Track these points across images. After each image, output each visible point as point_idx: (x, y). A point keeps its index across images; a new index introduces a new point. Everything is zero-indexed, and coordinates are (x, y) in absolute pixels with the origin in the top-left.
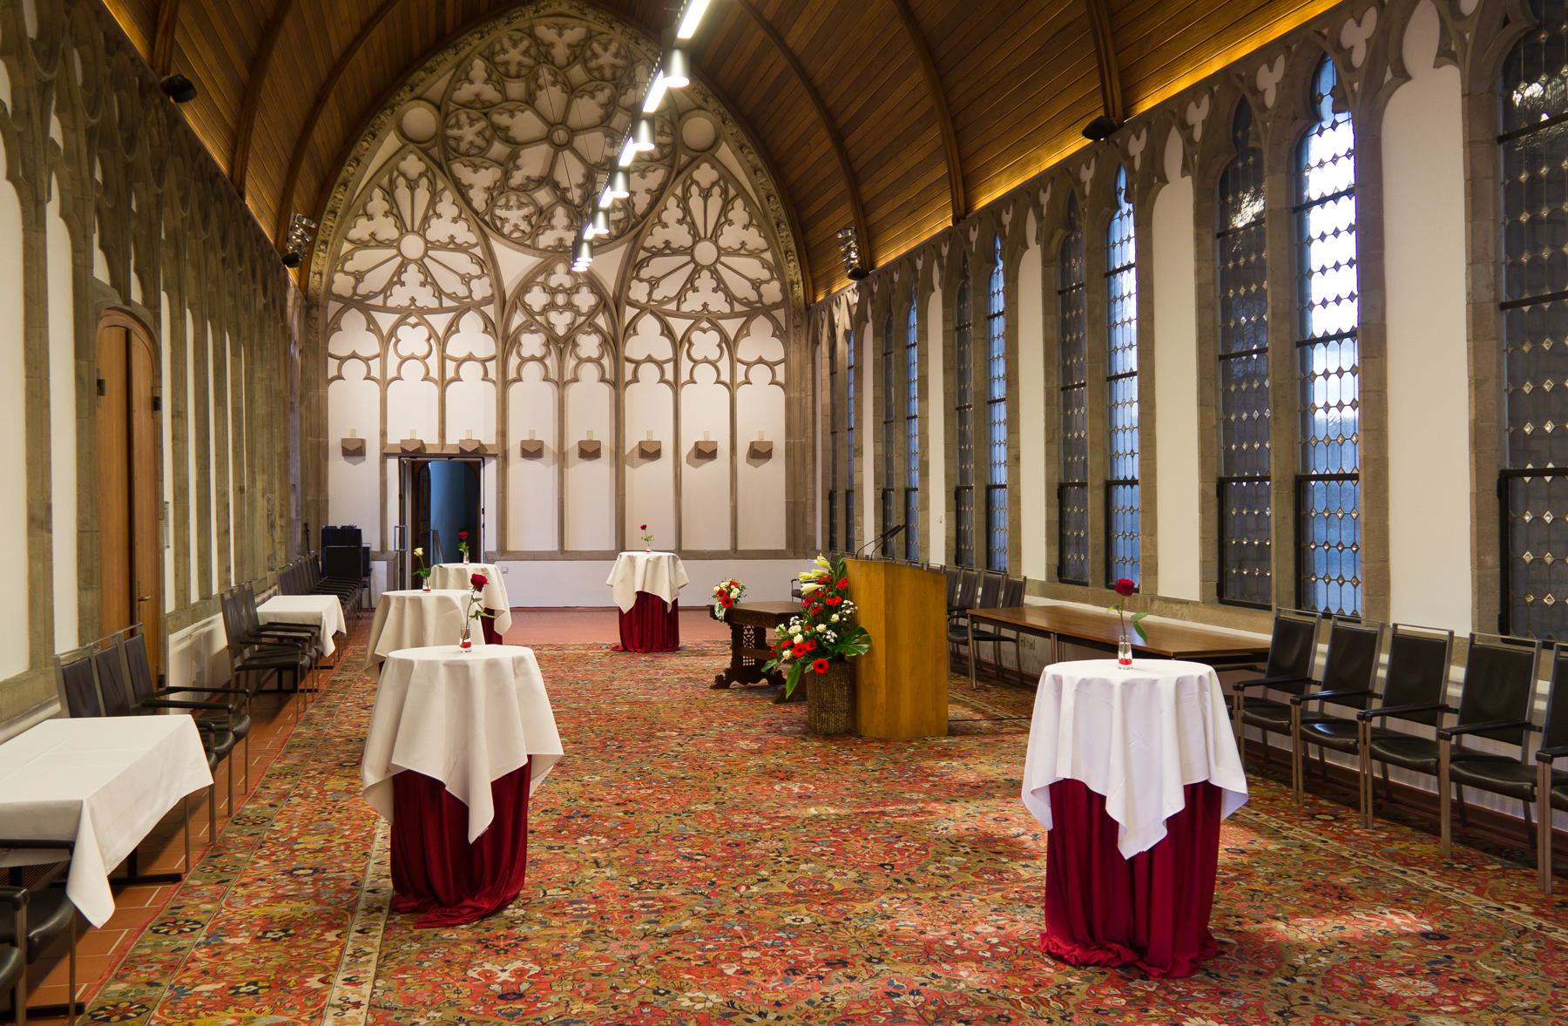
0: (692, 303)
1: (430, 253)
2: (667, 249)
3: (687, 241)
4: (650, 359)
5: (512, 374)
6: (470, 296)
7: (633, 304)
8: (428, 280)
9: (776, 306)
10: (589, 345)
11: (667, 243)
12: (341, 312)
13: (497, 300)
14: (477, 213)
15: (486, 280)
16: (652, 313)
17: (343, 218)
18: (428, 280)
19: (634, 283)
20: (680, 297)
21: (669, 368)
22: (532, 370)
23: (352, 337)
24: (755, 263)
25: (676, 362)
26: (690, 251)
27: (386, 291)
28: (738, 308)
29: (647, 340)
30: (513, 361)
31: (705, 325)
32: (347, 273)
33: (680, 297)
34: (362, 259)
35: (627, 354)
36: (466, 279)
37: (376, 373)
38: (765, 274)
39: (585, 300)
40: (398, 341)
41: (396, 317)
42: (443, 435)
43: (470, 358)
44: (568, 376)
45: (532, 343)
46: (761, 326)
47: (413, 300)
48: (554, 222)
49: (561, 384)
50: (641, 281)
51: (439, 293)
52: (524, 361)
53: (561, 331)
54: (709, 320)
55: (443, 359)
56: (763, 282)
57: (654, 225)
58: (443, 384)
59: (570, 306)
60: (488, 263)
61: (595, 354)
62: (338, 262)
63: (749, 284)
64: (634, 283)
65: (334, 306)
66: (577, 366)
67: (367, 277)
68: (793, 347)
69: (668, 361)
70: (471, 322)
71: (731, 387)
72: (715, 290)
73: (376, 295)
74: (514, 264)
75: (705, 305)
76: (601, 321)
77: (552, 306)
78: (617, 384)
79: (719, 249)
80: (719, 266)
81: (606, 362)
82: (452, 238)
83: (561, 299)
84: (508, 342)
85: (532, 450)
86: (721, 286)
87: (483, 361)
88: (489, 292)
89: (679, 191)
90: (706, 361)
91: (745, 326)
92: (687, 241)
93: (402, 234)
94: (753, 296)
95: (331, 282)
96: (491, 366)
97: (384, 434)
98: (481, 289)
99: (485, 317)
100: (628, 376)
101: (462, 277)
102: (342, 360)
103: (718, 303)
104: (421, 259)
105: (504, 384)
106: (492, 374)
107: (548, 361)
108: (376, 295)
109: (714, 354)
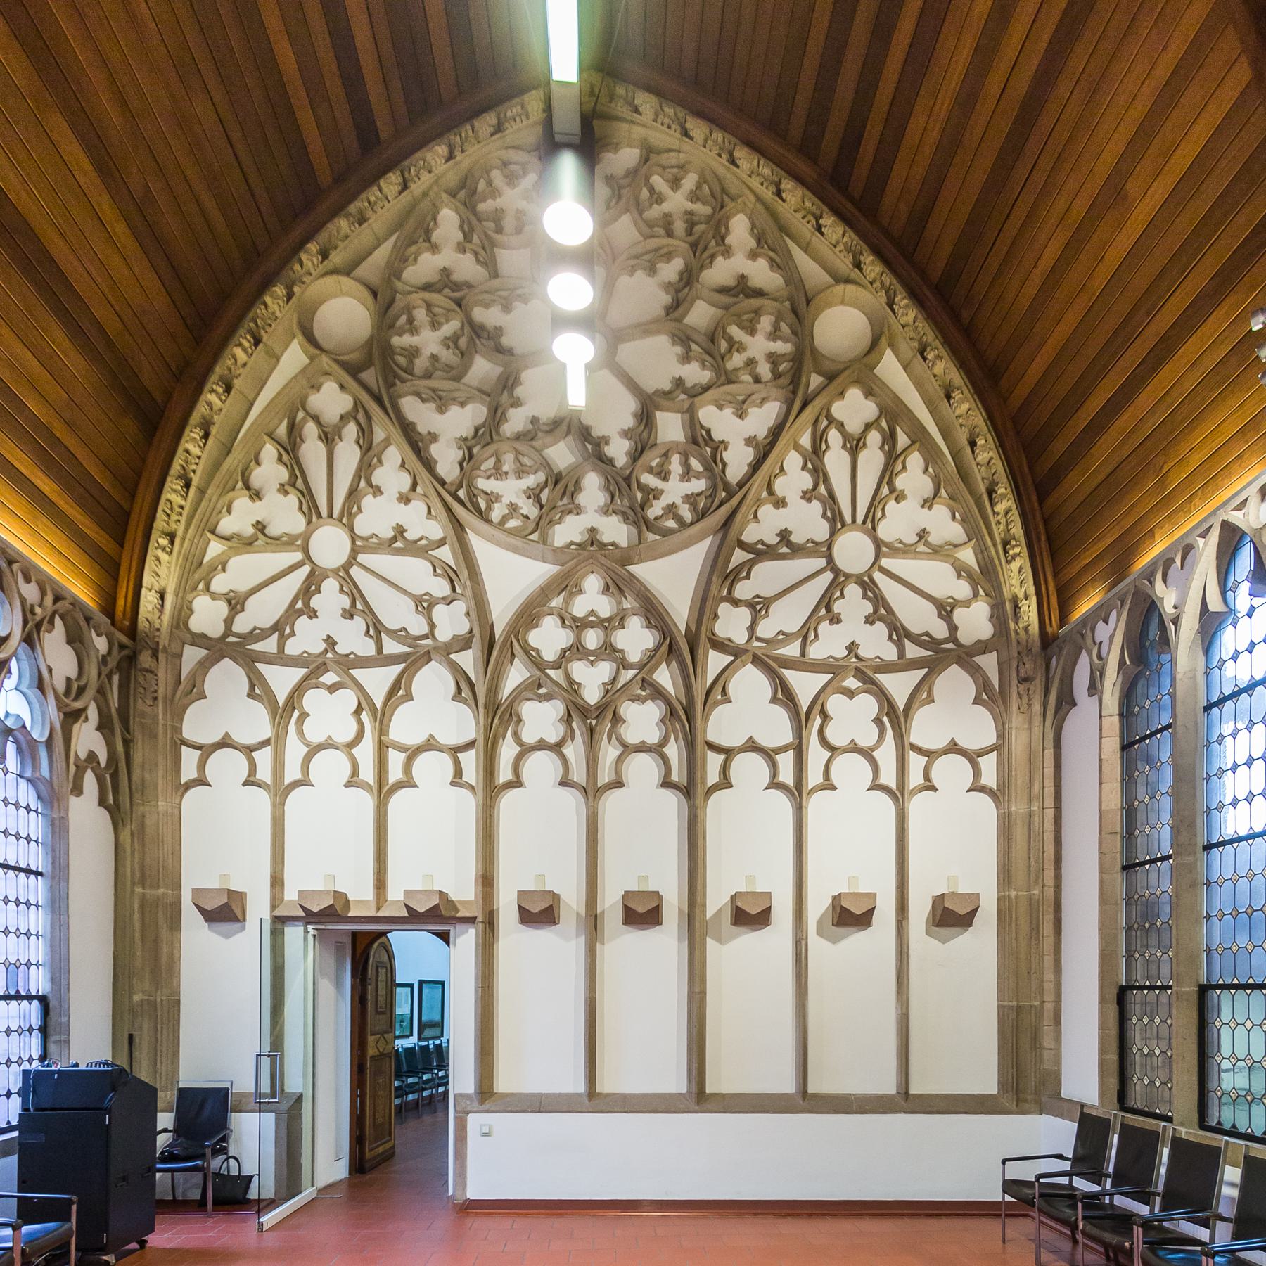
0: (830, 643)
1: (362, 558)
2: (785, 545)
3: (821, 531)
4: (752, 746)
5: (504, 774)
6: (431, 634)
7: (720, 645)
8: (357, 606)
9: (983, 647)
10: (642, 720)
11: (784, 535)
12: (204, 666)
13: (477, 642)
14: (443, 483)
15: (460, 606)
16: (757, 660)
17: (202, 492)
18: (357, 606)
19: (724, 608)
20: (806, 634)
21: (786, 762)
22: (541, 767)
23: (224, 708)
24: (945, 569)
25: (799, 750)
26: (825, 549)
27: (281, 628)
28: (913, 651)
29: (747, 711)
30: (507, 751)
31: (852, 683)
32: (214, 596)
33: (806, 634)
34: (243, 571)
35: (711, 737)
36: (425, 604)
37: (264, 773)
38: (962, 589)
39: (636, 639)
40: (304, 715)
41: (301, 672)
42: (381, 884)
43: (430, 745)
44: (604, 777)
45: (541, 719)
46: (954, 684)
47: (330, 642)
48: (581, 499)
49: (592, 792)
50: (736, 603)
51: (376, 629)
52: (526, 750)
53: (592, 695)
54: (859, 674)
55: (382, 748)
56: (955, 604)
57: (759, 502)
58: (383, 791)
59: (608, 650)
60: (465, 576)
61: (653, 737)
62: (197, 574)
63: (931, 609)
64: (724, 608)
65: (192, 655)
66: (620, 760)
67: (251, 603)
68: (1017, 720)
70: (433, 681)
71: (899, 795)
72: (870, 620)
73: (264, 634)
74: (509, 576)
75: (852, 647)
76: (665, 677)
77: (576, 650)
78: (691, 790)
79: (878, 543)
80: (877, 576)
81: (673, 751)
82: (400, 531)
83: (592, 639)
84: (498, 716)
85: (536, 908)
86: (881, 612)
87: (455, 751)
88: (463, 627)
89: (806, 441)
90: (854, 748)
92: (821, 531)
93: (309, 522)
94: (939, 630)
95: (183, 614)
96: (469, 760)
97: (277, 882)
98: (452, 621)
99: (456, 670)
100: (713, 777)
101: (418, 600)
102: (206, 751)
103: (875, 643)
104: (346, 567)
105: (491, 791)
106: (471, 773)
107: (569, 751)
108: (264, 634)
109: (868, 736)
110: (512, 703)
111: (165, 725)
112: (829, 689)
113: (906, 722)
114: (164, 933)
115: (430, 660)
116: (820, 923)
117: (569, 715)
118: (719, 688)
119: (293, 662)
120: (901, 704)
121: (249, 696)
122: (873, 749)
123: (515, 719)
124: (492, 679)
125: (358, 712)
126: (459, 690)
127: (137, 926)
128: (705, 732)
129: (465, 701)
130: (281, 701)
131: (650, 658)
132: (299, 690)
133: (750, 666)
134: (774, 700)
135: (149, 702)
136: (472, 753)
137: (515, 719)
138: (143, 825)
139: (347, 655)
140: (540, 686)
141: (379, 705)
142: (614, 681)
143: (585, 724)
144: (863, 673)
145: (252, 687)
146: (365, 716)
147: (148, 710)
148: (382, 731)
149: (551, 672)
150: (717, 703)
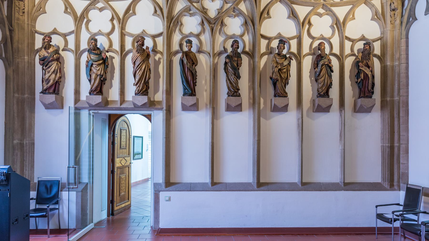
31: (321, 11)
35: (262, 32)
40: (89, 21)
53: (212, 14)
54: (324, 6)
55: (122, 35)
107: (202, 38)
110: (178, 17)
111: (28, 24)
112: (312, 13)
113: (344, 27)
114: (27, 114)
116: (308, 111)
117: (203, 22)
118: (266, 12)
120: (341, 20)
121: (65, 12)
122: (330, 38)
123: (180, 24)
124: (170, 6)
125: (112, 20)
126: (156, 11)
127: (16, 111)
129: (158, 16)
130: (79, 14)
132: (86, 11)
133: (279, 3)
134: (289, 17)
135: (21, 14)
136: (161, 38)
137: (180, 24)
138: (18, 67)
140: (190, 10)
141: (121, 16)
142: (222, 8)
143: (209, 26)
144: (326, 6)
145: (66, 8)
146: (115, 22)
147: (21, 17)
148: (123, 28)
149: (195, 4)
150: (265, 18)
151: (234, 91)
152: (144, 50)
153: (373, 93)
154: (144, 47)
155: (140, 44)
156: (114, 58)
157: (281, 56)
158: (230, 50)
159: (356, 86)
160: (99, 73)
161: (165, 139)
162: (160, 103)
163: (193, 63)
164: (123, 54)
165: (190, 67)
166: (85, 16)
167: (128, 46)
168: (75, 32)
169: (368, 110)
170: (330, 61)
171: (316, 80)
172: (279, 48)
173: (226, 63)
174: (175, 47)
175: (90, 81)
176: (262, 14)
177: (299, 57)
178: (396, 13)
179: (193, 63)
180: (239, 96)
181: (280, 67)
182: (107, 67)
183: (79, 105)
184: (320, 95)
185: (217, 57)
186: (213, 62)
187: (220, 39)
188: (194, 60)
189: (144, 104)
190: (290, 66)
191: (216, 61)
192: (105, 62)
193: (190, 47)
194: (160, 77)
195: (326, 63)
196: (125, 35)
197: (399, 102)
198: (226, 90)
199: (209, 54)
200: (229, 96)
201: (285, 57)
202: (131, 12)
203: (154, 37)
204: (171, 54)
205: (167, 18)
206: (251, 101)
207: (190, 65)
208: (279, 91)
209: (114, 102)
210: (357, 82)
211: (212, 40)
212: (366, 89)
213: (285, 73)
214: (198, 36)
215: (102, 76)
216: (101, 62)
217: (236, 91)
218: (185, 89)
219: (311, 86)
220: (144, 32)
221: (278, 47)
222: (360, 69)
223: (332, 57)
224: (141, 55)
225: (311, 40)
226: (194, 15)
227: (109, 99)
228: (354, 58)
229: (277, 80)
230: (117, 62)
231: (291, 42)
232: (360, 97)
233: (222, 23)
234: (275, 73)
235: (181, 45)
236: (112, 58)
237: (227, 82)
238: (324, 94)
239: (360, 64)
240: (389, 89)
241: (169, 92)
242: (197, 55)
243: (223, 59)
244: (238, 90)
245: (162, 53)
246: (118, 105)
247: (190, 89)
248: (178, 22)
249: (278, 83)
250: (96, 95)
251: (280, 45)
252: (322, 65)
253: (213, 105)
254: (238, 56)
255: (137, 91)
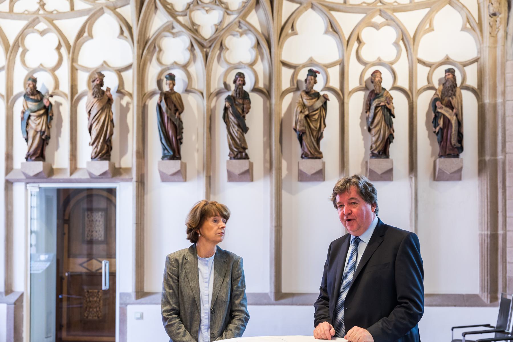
31: (378, 19)
35: (285, 58)
41: (23, 23)
53: (207, 32)
55: (73, 71)
69: (333, 65)
70: (107, 26)
91: (428, 19)
107: (192, 69)
110: (155, 40)
115: (103, 13)
117: (192, 46)
118: (289, 25)
119: (20, 16)
122: (392, 63)
125: (58, 48)
126: (122, 32)
128: (280, 55)
130: (11, 42)
131: (244, 7)
132: (22, 36)
134: (326, 32)
137: (157, 49)
139: (52, 12)
140: (173, 28)
141: (72, 42)
143: (202, 51)
144: (385, 13)
146: (63, 50)
148: (73, 60)
150: (288, 36)
151: (239, 151)
152: (103, 92)
153: (461, 149)
154: (104, 88)
155: (97, 85)
156: (61, 104)
157: (310, 96)
158: (233, 87)
159: (435, 138)
160: (39, 129)
161: (135, 226)
162: (128, 170)
163: (177, 110)
164: (74, 98)
165: (171, 115)
166: (20, 44)
167: (83, 85)
168: (6, 68)
169: (457, 175)
170: (390, 99)
171: (370, 130)
172: (308, 82)
173: (226, 109)
174: (151, 85)
175: (27, 140)
176: (282, 29)
177: (341, 95)
178: (498, 19)
179: (177, 110)
180: (247, 157)
181: (307, 113)
182: (51, 118)
183: (10, 177)
184: (373, 155)
185: (215, 99)
186: (208, 106)
187: (219, 70)
188: (177, 105)
189: (104, 174)
190: (325, 109)
191: (213, 104)
192: (47, 112)
193: (171, 85)
194: (128, 131)
195: (382, 104)
196: (77, 70)
197: (504, 163)
198: (228, 151)
199: (202, 94)
200: (231, 158)
201: (317, 95)
202: (86, 34)
203: (119, 72)
204: (144, 96)
205: (138, 42)
206: (268, 165)
207: (171, 114)
208: (306, 150)
209: (60, 170)
210: (435, 132)
211: (205, 74)
212: (448, 143)
213: (316, 120)
214: (185, 67)
215: (44, 132)
216: (42, 112)
217: (242, 150)
218: (164, 149)
219: (364, 139)
220: (105, 65)
221: (306, 80)
222: (438, 112)
223: (394, 94)
224: (99, 100)
225: (362, 67)
226: (180, 35)
227: (55, 167)
228: (433, 92)
229: (304, 133)
230: (65, 111)
231: (330, 70)
232: (440, 156)
233: (221, 45)
234: (300, 122)
235: (159, 83)
236: (59, 104)
237: (228, 138)
238: (379, 152)
239: (438, 104)
240: (488, 143)
241: (142, 154)
242: (184, 97)
243: (222, 103)
244: (245, 148)
245: (131, 95)
246: (67, 176)
247: (173, 148)
248: (155, 47)
249: (304, 138)
250: (35, 160)
251: (309, 77)
252: (376, 107)
253: (207, 172)
254: (245, 96)
255: (93, 154)
